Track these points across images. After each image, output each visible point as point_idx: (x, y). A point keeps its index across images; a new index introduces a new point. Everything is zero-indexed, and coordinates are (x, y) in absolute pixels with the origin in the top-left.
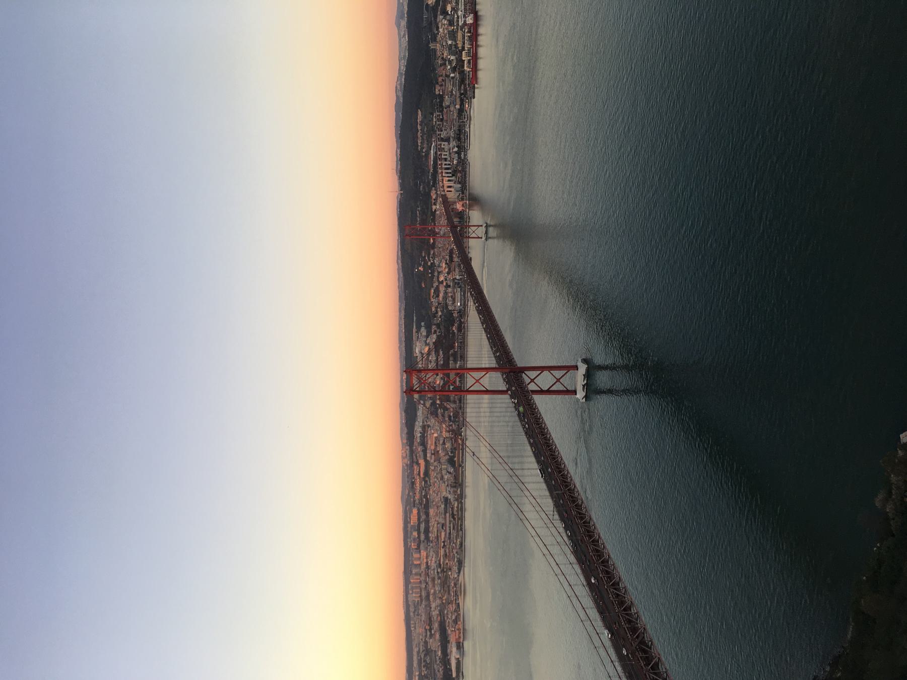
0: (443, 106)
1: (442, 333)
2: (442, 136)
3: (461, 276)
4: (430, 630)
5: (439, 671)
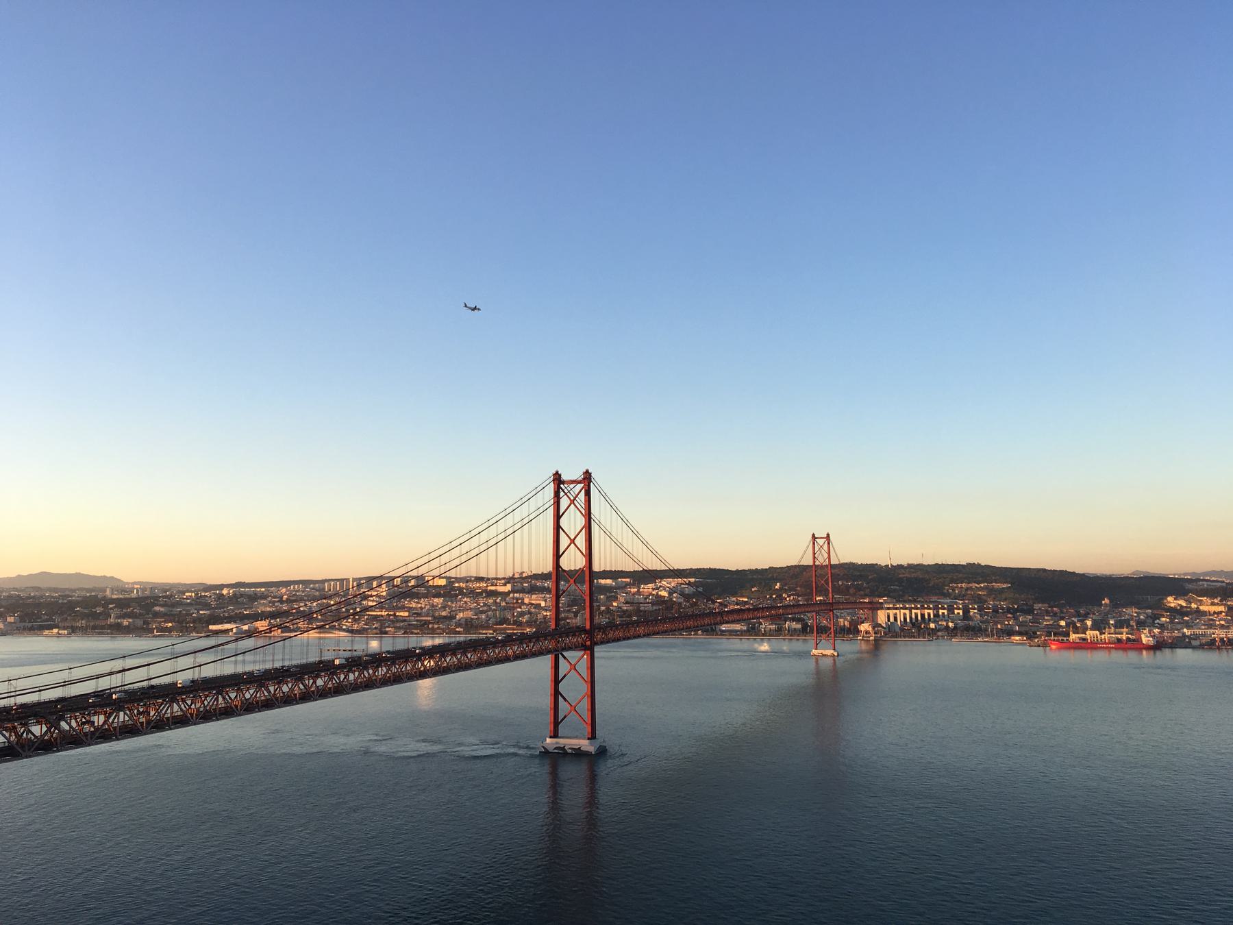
1: (683, 608)
3: (765, 630)
4: (281, 601)
5: (225, 611)
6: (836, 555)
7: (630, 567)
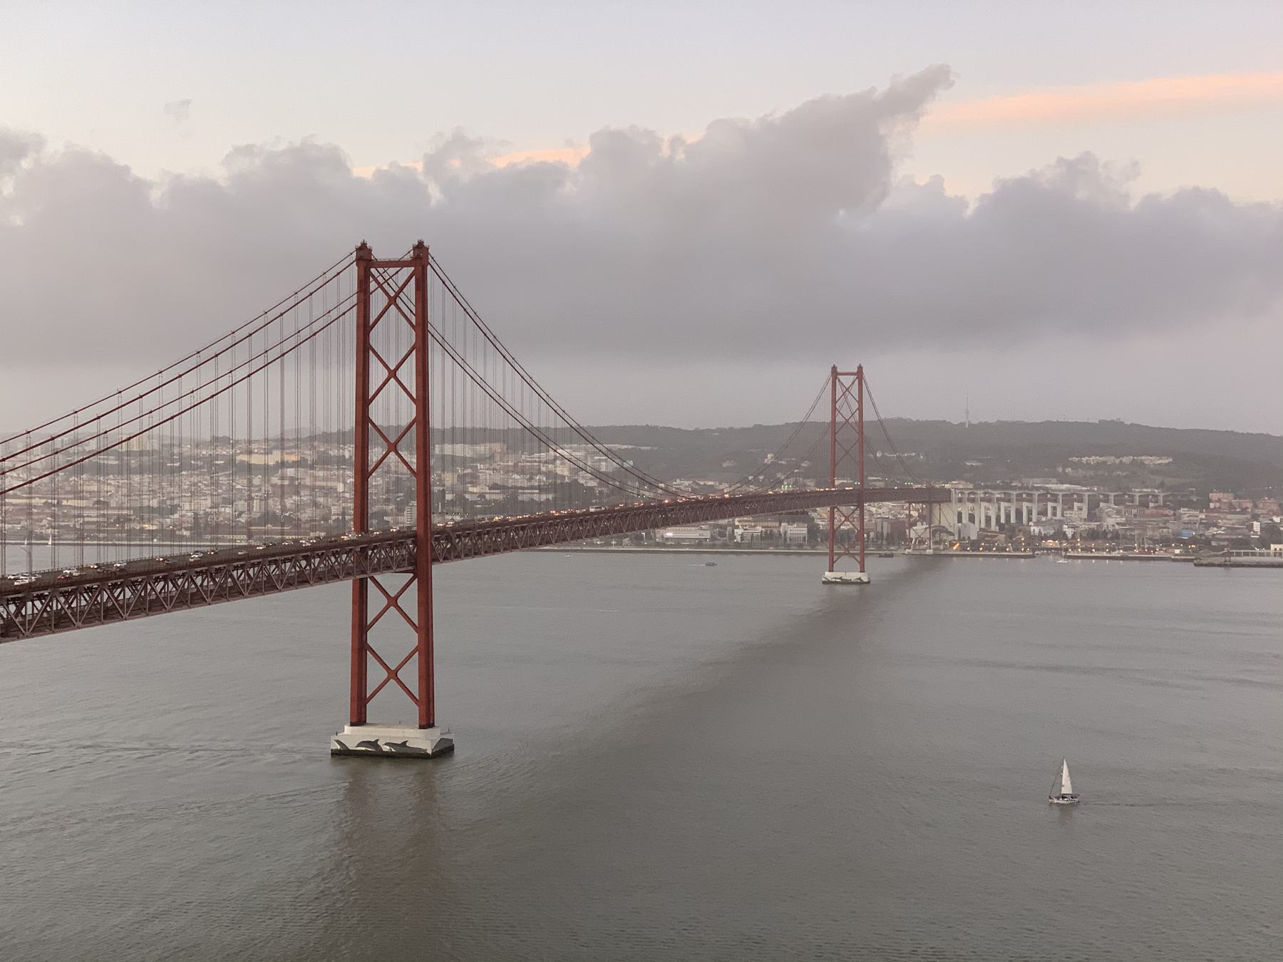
0: (1179, 509)
1: (596, 497)
2: (1102, 504)
6: (874, 404)
7: (500, 421)
